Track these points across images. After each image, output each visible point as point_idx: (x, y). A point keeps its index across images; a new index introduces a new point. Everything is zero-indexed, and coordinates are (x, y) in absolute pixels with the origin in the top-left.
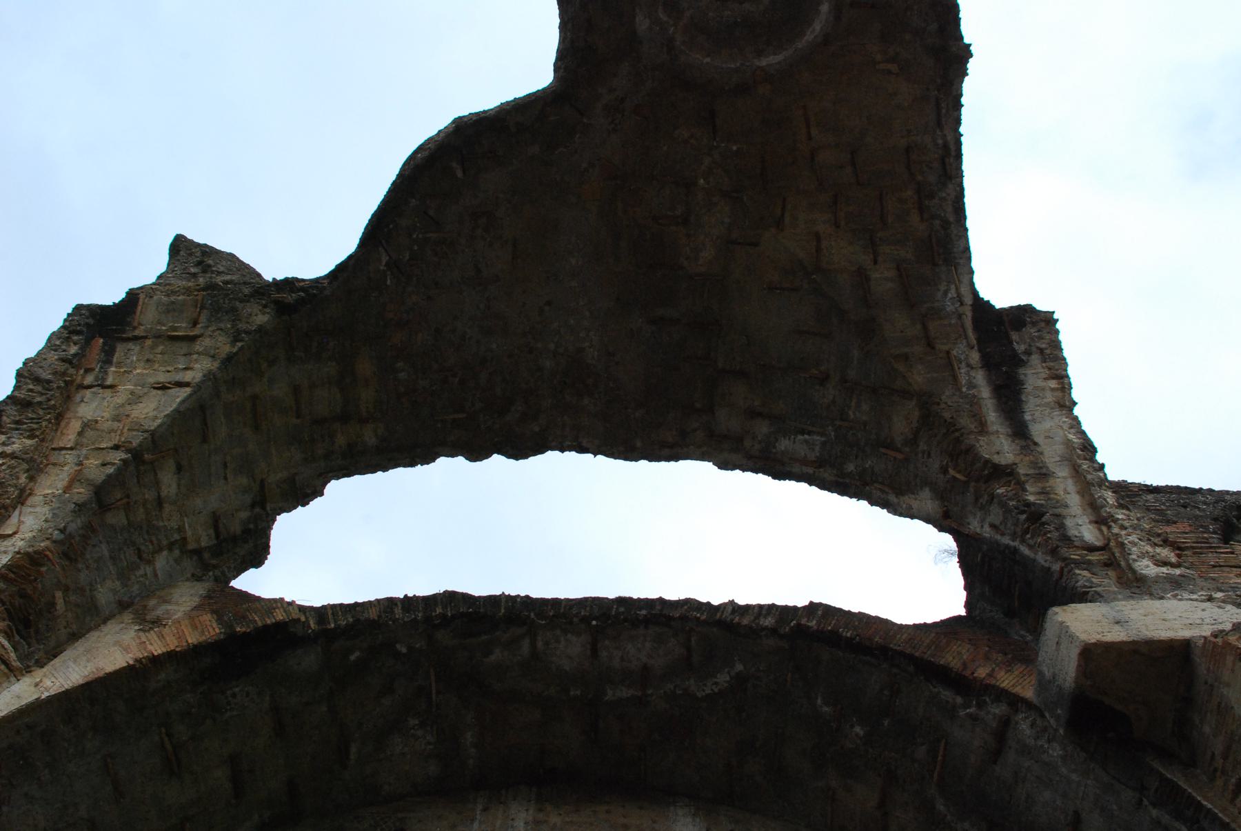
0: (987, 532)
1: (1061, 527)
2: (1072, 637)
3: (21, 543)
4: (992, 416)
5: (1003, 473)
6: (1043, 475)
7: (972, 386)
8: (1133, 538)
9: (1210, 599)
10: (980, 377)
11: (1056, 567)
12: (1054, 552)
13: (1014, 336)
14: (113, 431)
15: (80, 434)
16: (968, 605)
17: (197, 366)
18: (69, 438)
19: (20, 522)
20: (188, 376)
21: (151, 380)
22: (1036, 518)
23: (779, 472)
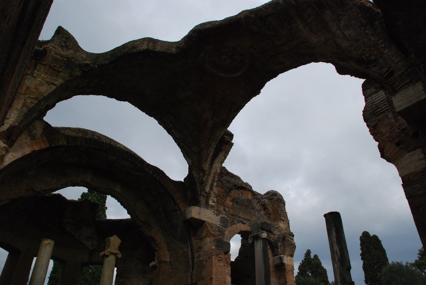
0: (195, 176)
1: (205, 187)
2: (191, 214)
3: (11, 122)
4: (209, 159)
5: (204, 171)
6: (209, 175)
7: (210, 151)
8: (212, 196)
9: (214, 212)
10: (213, 150)
11: (199, 193)
12: (201, 191)
13: (224, 146)
14: (34, 93)
15: (26, 91)
16: (185, 179)
17: (59, 80)
18: (23, 91)
19: (11, 115)
20: (56, 83)
21: (46, 80)
22: (203, 183)
23: (169, 132)
